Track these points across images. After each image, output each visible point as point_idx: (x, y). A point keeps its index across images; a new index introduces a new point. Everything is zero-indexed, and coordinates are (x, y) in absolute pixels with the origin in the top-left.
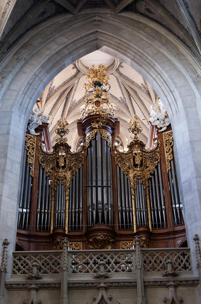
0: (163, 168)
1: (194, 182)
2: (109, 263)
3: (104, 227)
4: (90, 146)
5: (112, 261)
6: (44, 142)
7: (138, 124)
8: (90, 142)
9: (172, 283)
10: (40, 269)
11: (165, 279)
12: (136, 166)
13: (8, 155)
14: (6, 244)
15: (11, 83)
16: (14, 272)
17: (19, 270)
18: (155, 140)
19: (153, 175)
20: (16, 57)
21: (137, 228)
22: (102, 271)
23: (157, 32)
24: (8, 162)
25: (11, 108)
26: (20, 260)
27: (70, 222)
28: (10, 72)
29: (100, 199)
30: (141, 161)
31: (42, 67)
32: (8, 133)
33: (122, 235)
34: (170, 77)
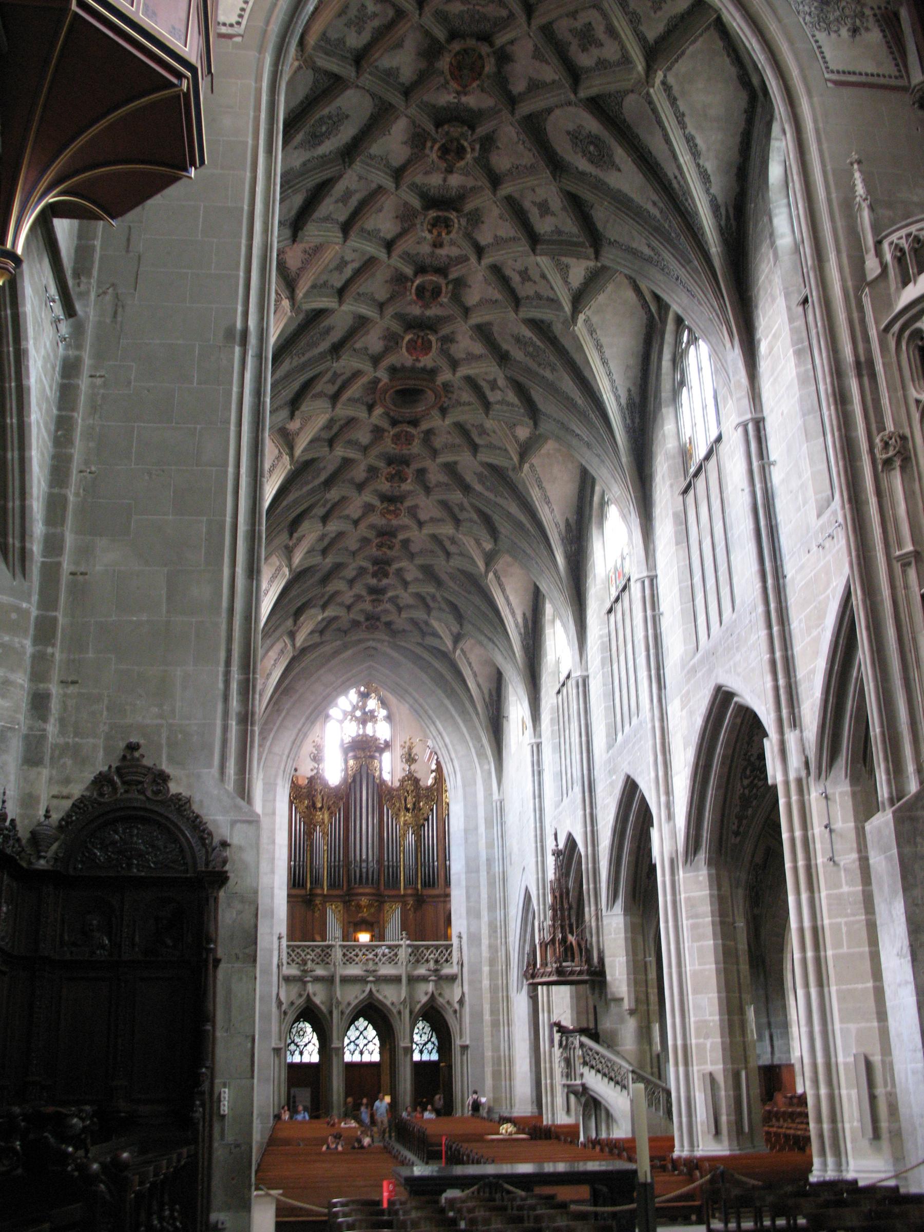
0: (439, 812)
1: (463, 877)
2: (376, 955)
3: (367, 890)
4: (354, 781)
7: (414, 751)
9: (433, 978)
10: (313, 960)
11: (428, 973)
12: (407, 810)
13: (277, 841)
14: (280, 938)
15: (271, 744)
16: (288, 963)
17: (293, 961)
18: (432, 771)
19: (428, 820)
20: (276, 707)
21: (405, 888)
22: (371, 966)
23: (442, 676)
24: (277, 847)
25: (275, 780)
26: (293, 951)
27: (329, 874)
28: (271, 730)
29: (364, 857)
30: (414, 804)
31: (307, 719)
32: (274, 813)
33: (389, 896)
34: (451, 742)
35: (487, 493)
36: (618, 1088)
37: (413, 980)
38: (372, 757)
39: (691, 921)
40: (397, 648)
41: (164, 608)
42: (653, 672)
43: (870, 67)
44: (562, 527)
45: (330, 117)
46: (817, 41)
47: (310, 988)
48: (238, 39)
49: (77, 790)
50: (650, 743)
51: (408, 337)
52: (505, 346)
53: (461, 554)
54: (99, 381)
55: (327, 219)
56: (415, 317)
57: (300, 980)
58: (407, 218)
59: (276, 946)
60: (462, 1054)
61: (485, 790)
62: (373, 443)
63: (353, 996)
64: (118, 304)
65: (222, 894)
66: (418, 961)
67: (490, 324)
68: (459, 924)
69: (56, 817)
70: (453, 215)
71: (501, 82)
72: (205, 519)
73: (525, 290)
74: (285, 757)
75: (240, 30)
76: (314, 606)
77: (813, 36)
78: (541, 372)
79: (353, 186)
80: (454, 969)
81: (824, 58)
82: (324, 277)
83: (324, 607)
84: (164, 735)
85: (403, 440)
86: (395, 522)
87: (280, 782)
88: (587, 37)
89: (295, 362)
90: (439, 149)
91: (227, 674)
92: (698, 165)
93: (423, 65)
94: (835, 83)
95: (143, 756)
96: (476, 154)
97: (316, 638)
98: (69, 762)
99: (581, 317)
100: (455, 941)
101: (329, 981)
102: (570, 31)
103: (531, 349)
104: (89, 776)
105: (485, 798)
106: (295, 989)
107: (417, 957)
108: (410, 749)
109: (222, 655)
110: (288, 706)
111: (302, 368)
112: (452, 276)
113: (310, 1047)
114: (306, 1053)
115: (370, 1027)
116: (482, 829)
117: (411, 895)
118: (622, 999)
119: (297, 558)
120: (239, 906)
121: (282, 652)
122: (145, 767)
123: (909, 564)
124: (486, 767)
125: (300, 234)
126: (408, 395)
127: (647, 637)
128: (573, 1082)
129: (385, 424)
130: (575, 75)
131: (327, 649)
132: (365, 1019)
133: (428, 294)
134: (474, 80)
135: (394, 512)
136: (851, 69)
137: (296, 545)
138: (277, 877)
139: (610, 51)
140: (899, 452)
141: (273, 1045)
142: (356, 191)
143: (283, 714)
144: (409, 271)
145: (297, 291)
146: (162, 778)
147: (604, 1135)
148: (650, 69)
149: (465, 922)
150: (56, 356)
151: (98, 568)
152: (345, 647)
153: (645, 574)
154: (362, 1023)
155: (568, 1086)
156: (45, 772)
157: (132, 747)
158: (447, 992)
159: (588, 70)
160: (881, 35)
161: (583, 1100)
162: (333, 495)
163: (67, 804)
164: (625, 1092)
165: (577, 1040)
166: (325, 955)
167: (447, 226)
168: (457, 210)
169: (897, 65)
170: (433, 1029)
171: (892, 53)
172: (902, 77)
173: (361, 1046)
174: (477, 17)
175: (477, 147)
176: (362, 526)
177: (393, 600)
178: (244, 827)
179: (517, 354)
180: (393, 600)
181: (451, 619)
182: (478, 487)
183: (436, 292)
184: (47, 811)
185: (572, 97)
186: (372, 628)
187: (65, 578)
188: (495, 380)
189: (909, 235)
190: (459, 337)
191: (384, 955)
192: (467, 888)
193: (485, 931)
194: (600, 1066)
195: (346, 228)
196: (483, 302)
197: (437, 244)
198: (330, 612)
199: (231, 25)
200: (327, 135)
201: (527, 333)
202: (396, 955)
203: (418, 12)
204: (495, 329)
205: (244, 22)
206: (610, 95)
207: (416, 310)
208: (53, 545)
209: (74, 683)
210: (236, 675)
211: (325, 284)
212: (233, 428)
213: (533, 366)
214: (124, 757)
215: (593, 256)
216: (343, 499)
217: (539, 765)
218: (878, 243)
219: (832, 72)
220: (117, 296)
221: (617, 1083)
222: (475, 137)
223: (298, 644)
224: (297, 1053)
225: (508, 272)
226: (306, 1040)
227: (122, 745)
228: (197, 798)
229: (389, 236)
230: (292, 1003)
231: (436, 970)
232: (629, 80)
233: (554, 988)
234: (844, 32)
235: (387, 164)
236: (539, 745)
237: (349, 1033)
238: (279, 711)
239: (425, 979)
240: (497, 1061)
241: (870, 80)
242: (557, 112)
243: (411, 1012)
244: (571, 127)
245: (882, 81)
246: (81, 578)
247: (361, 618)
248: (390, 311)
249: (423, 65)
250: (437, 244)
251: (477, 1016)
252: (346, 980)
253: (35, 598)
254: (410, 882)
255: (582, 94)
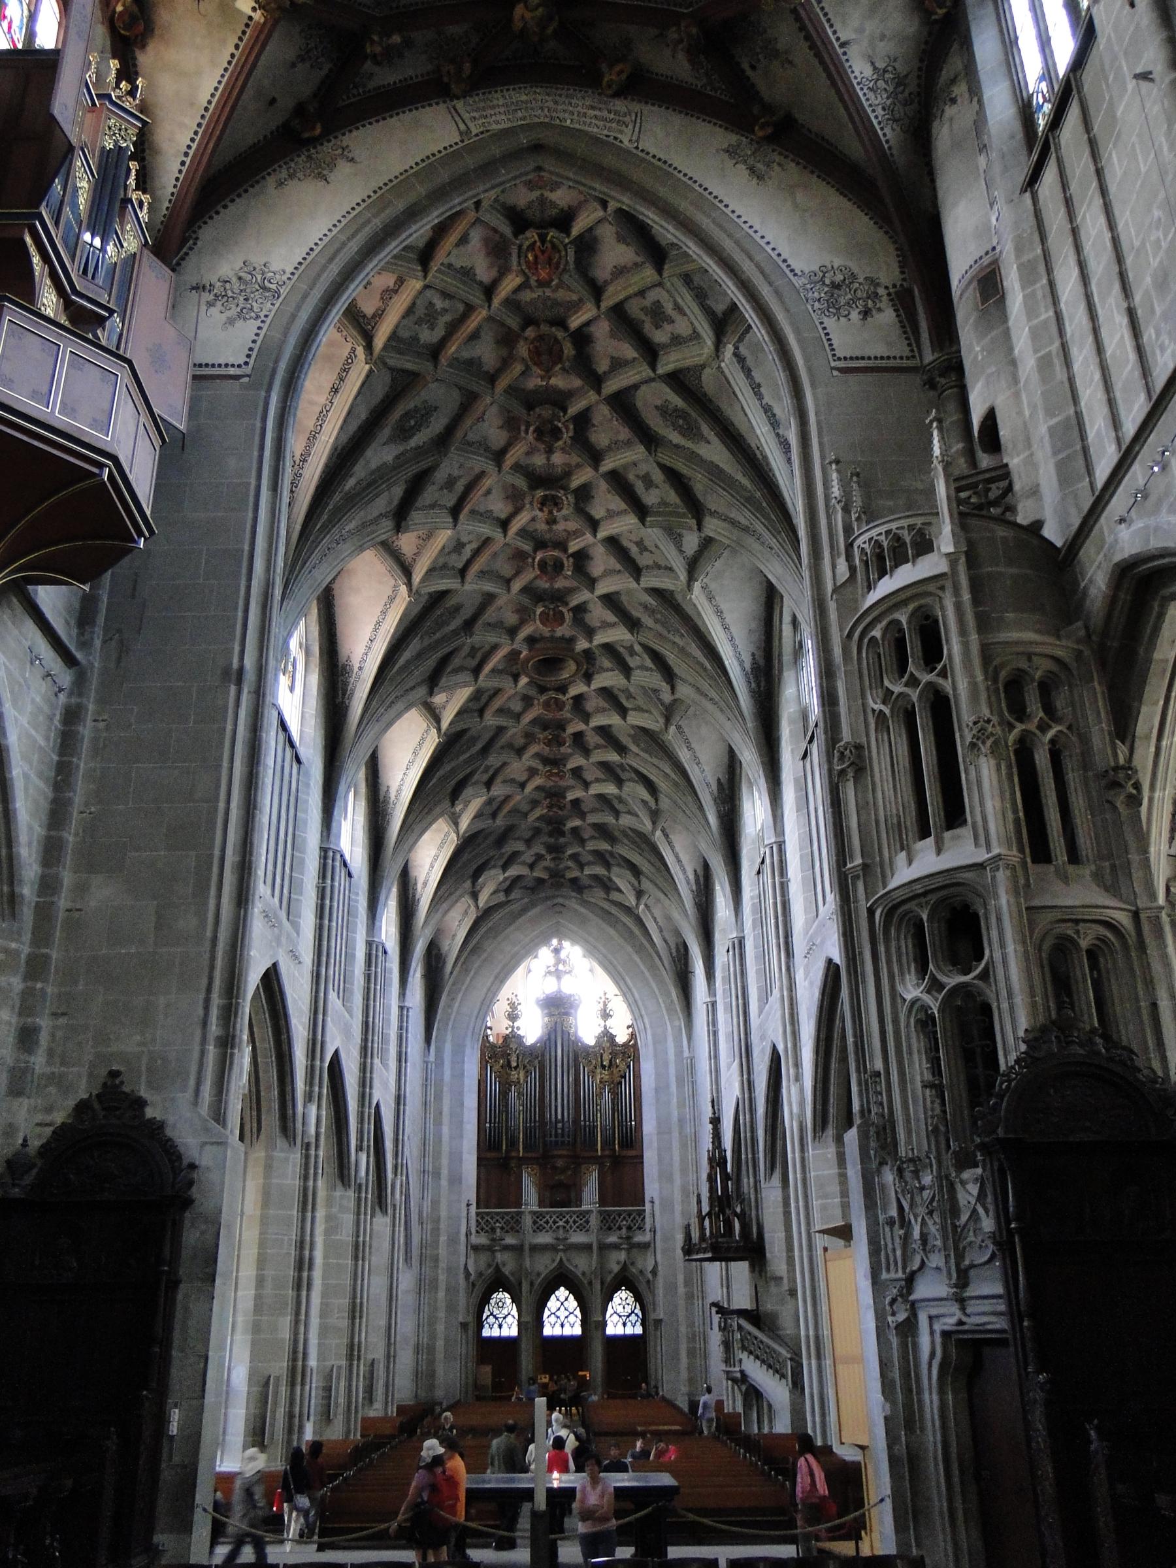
1: (655, 1138)
2: (567, 1222)
3: (565, 1153)
4: (549, 1039)
5: (571, 1221)
6: (490, 1028)
7: (610, 1006)
8: (549, 1034)
10: (502, 1228)
11: (620, 1241)
12: (603, 1067)
13: (465, 1104)
14: (468, 1205)
23: (631, 932)
26: (482, 1218)
27: (525, 1134)
28: (460, 990)
29: (559, 1117)
30: (611, 1061)
31: (496, 977)
32: (462, 1075)
35: (642, 754)
36: (777, 1376)
37: (604, 1248)
38: (567, 1014)
39: (820, 1202)
40: (585, 903)
41: (151, 941)
42: (782, 940)
43: (880, 350)
44: (714, 787)
45: (416, 409)
46: (824, 328)
47: (500, 1257)
48: (246, 380)
49: (59, 1118)
50: (779, 1014)
51: (539, 610)
52: (636, 613)
53: (629, 813)
54: (101, 725)
55: (433, 506)
56: (545, 590)
57: (489, 1249)
58: (515, 498)
59: (464, 1214)
60: (656, 1329)
61: (676, 1047)
62: (525, 710)
63: (544, 1265)
64: (124, 649)
65: (187, 1214)
66: (610, 1229)
67: (617, 593)
68: (652, 1188)
69: (35, 1144)
70: (561, 493)
71: (584, 365)
72: (193, 853)
73: (643, 560)
74: (473, 1019)
75: (248, 370)
76: (494, 867)
77: (821, 323)
78: (671, 637)
79: (456, 473)
80: (645, 1237)
81: (831, 345)
82: (441, 561)
83: (505, 867)
84: (144, 1060)
85: (554, 706)
86: (562, 783)
87: (468, 1042)
88: (658, 314)
89: (426, 642)
90: (535, 431)
91: (207, 1002)
92: (778, 435)
93: (504, 352)
94: (842, 370)
95: (122, 1083)
96: (571, 434)
97: (501, 897)
98: (52, 1090)
99: (697, 586)
100: (648, 1206)
101: (518, 1249)
102: (642, 310)
103: (659, 616)
104: (71, 1103)
105: (676, 1055)
106: (484, 1258)
107: (608, 1223)
108: (605, 1005)
109: (204, 981)
110: (476, 966)
111: (432, 647)
112: (570, 551)
113: (509, 1319)
114: (505, 1326)
115: (571, 1297)
116: (673, 1088)
117: (609, 1156)
118: (781, 1278)
119: (464, 823)
120: (203, 1227)
121: (466, 912)
122: (124, 1093)
123: (858, 877)
124: (677, 1023)
125: (403, 524)
126: (550, 664)
127: (775, 904)
128: (732, 1369)
129: (532, 692)
130: (651, 352)
131: (515, 907)
132: (567, 1288)
133: (553, 568)
134: (555, 364)
135: (557, 774)
136: (858, 353)
137: (462, 811)
138: (465, 1142)
139: (682, 327)
140: (852, 763)
141: (461, 1319)
142: (460, 477)
143: (472, 973)
144: (527, 547)
145: (414, 576)
146: (141, 1103)
147: (766, 1430)
148: (718, 344)
149: (657, 1186)
150: (53, 707)
151: (93, 904)
152: (533, 904)
153: (773, 840)
154: (562, 1292)
155: (728, 1372)
156: (25, 1102)
157: (114, 1074)
158: (640, 1265)
159: (664, 346)
160: (894, 314)
161: (744, 1388)
162: (493, 760)
163: (48, 1131)
164: (784, 1381)
165: (735, 1322)
166: (515, 1224)
167: (556, 504)
168: (565, 488)
169: (909, 345)
170: (636, 1300)
171: (905, 332)
172: (914, 357)
173: (562, 1318)
174: (549, 303)
175: (571, 427)
176: (529, 788)
177: (575, 857)
178: (214, 1148)
179: (647, 621)
180: (575, 857)
181: (628, 874)
182: (634, 748)
183: (558, 567)
184: (25, 1140)
185: (652, 375)
186: (558, 886)
187: (61, 915)
188: (632, 646)
189: (888, 532)
190: (591, 606)
191: (575, 1222)
192: (659, 1149)
193: (677, 1196)
194: (758, 1352)
195: (455, 512)
196: (608, 573)
197: (552, 521)
198: (513, 871)
199: (239, 366)
200: (418, 428)
201: (651, 601)
202: (587, 1222)
203: (487, 305)
204: (624, 598)
205: (252, 361)
206: (688, 369)
207: (543, 584)
208: (48, 885)
209: (64, 1014)
210: (216, 1000)
211: (444, 566)
212: (225, 764)
213: (665, 633)
214: (105, 1084)
215: (696, 527)
216: (504, 764)
217: (714, 1025)
218: (849, 546)
219: (839, 359)
220: (121, 641)
221: (777, 1371)
222: (566, 418)
223: (481, 904)
224: (496, 1326)
225: (625, 543)
226: (505, 1312)
227: (103, 1072)
228: (171, 1120)
229: (503, 516)
230: (480, 1274)
231: (629, 1238)
232: (700, 355)
233: (706, 1264)
234: (855, 315)
235: (487, 449)
236: (714, 1004)
237: (549, 1304)
238: (467, 971)
239: (616, 1247)
240: (692, 1338)
241: (884, 363)
242: (643, 388)
243: (602, 1283)
244: (659, 403)
245: (892, 363)
246: (76, 915)
247: (545, 876)
248: (517, 586)
249: (504, 352)
250: (552, 521)
251: (672, 1288)
252: (535, 1248)
253: (27, 937)
254: (608, 1143)
255: (660, 371)
